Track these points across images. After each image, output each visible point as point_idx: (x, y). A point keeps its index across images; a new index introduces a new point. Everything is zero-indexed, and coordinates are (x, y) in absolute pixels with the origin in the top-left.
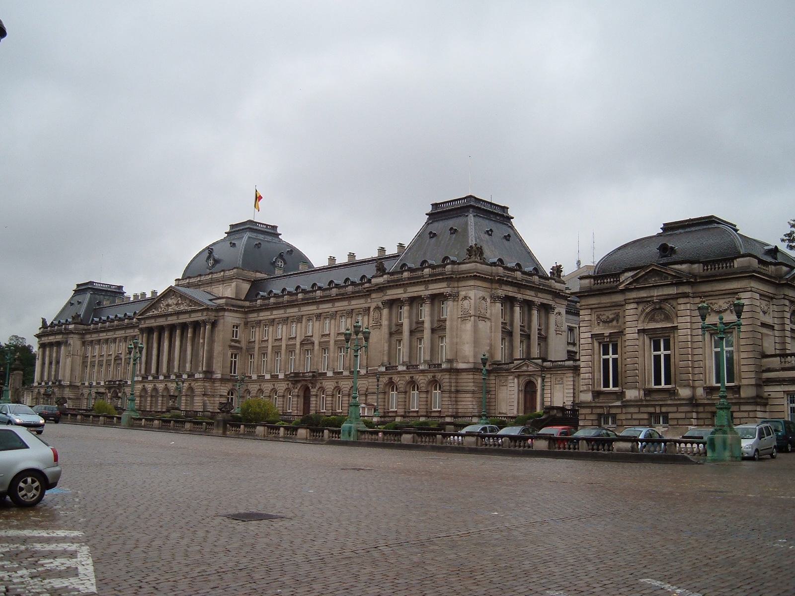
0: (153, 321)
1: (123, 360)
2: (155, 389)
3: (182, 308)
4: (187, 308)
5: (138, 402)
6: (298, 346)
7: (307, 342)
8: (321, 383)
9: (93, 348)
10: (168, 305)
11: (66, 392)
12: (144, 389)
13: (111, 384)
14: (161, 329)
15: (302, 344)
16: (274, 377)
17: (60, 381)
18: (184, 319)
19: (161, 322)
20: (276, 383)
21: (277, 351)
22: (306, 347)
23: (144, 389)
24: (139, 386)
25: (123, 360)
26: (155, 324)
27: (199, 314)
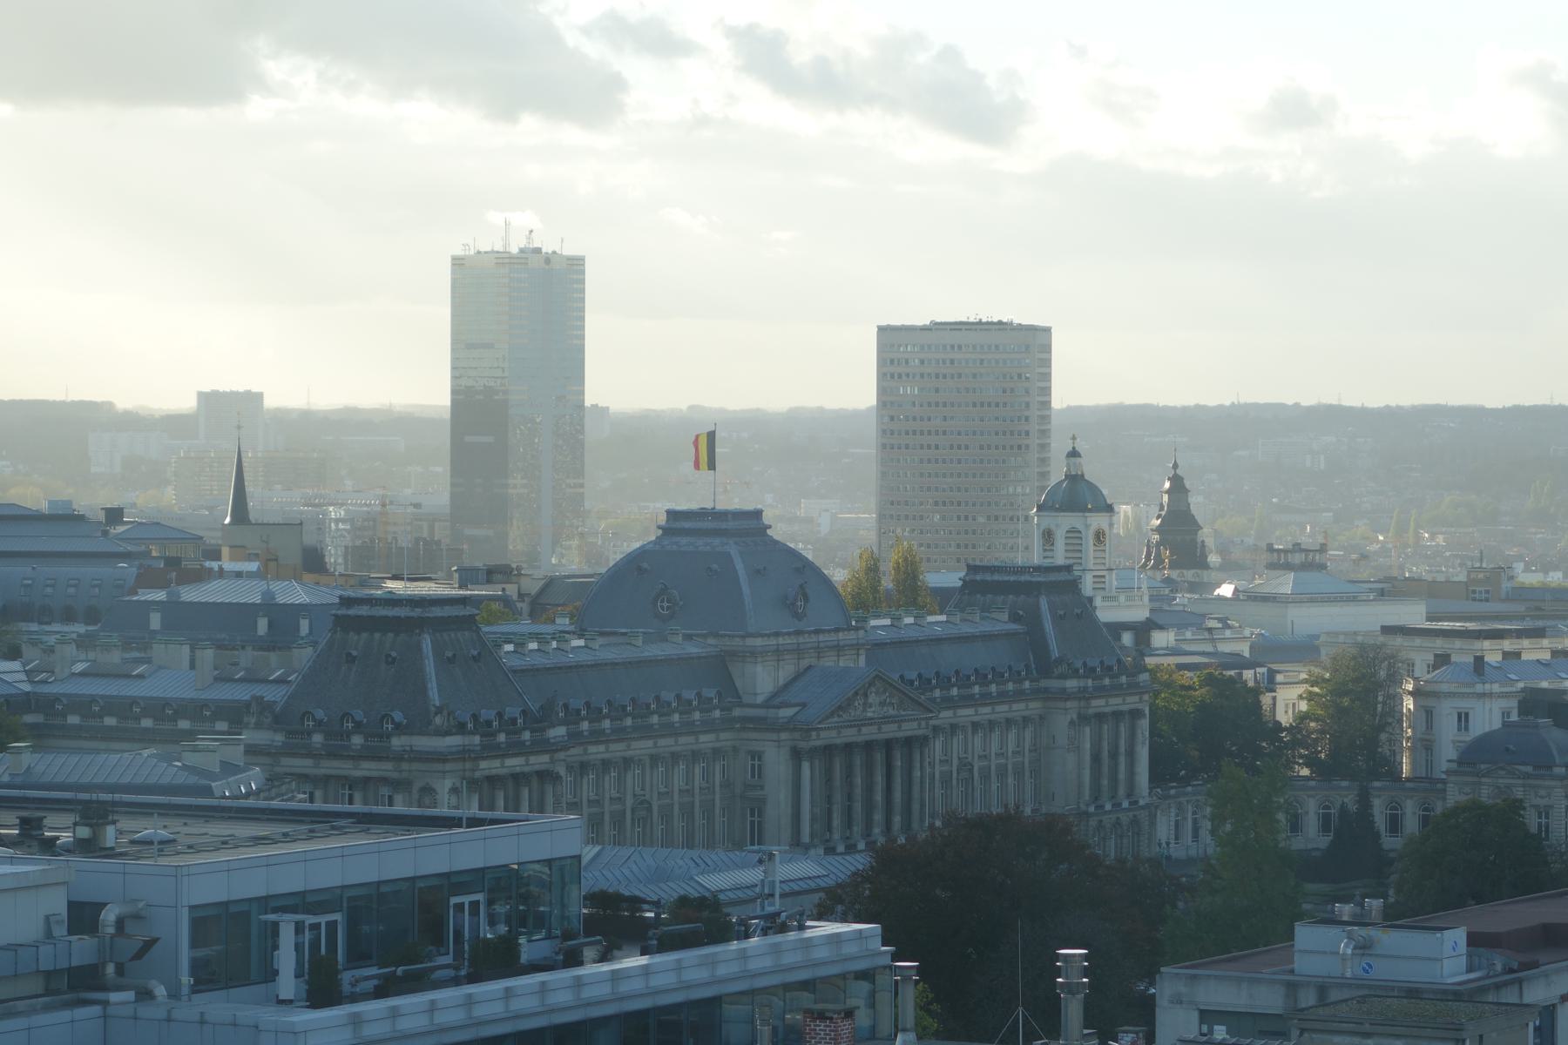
18: (890, 731)
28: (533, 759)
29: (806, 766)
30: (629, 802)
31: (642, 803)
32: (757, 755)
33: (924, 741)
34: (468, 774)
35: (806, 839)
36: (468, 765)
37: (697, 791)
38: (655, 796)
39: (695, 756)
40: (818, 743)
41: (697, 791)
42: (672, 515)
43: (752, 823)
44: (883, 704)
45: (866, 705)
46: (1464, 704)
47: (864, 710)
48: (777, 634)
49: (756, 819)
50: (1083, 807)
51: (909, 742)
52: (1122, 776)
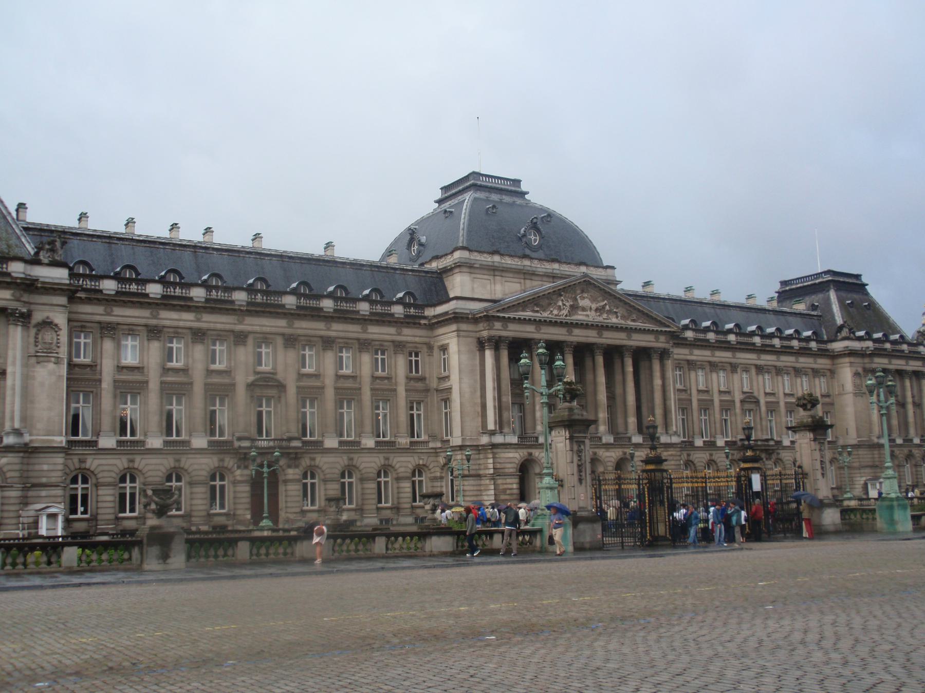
0: (531, 328)
1: (292, 391)
3: (614, 320)
4: (623, 322)
5: (515, 486)
6: (738, 404)
7: (750, 400)
8: (778, 454)
9: (118, 347)
10: (574, 308)
11: (45, 467)
15: (742, 402)
16: (710, 445)
17: (18, 433)
20: (714, 452)
21: (706, 406)
22: (747, 406)
25: (292, 391)
27: (651, 337)
33: (664, 354)
35: (491, 426)
43: (446, 413)
44: (599, 310)
51: (641, 355)
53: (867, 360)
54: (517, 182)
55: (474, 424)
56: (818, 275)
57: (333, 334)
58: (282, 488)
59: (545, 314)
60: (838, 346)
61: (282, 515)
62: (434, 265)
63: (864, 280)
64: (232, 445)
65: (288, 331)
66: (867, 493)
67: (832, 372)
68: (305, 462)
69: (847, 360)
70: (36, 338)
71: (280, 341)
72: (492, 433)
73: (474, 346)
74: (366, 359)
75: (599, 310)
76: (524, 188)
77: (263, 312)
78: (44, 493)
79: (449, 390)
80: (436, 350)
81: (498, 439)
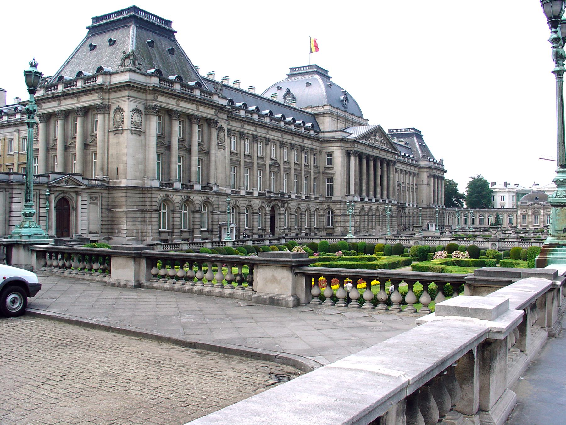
0: (363, 148)
2: (370, 209)
3: (384, 147)
12: (363, 209)
13: (278, 197)
14: (368, 157)
18: (383, 155)
19: (369, 151)
23: (363, 209)
24: (358, 206)
26: (365, 152)
27: (391, 155)
28: (201, 109)
29: (352, 159)
30: (268, 162)
31: (275, 163)
32: (330, 154)
33: (394, 163)
34: (150, 103)
35: (352, 192)
36: (150, 97)
37: (303, 166)
38: (282, 162)
39: (303, 149)
40: (358, 150)
41: (303, 166)
42: (293, 69)
43: (328, 185)
44: (381, 141)
45: (376, 140)
46: (503, 194)
47: (375, 142)
48: (337, 109)
49: (330, 183)
50: (432, 206)
51: (389, 163)
52: (440, 198)
53: (431, 170)
54: (327, 71)
55: (344, 191)
56: (407, 130)
57: (294, 142)
58: (277, 218)
59: (368, 142)
60: (422, 163)
61: (277, 230)
62: (309, 110)
63: (422, 134)
64: (265, 195)
65: (281, 139)
66: (428, 229)
67: (418, 174)
68: (286, 205)
69: (426, 170)
70: (218, 136)
71: (278, 144)
72: (354, 196)
73: (345, 153)
74: (303, 155)
75: (381, 141)
76: (330, 74)
77: (276, 129)
78: (220, 216)
79: (333, 174)
80: (323, 154)
81: (356, 199)
